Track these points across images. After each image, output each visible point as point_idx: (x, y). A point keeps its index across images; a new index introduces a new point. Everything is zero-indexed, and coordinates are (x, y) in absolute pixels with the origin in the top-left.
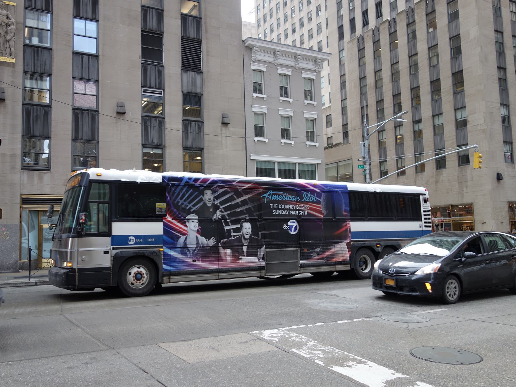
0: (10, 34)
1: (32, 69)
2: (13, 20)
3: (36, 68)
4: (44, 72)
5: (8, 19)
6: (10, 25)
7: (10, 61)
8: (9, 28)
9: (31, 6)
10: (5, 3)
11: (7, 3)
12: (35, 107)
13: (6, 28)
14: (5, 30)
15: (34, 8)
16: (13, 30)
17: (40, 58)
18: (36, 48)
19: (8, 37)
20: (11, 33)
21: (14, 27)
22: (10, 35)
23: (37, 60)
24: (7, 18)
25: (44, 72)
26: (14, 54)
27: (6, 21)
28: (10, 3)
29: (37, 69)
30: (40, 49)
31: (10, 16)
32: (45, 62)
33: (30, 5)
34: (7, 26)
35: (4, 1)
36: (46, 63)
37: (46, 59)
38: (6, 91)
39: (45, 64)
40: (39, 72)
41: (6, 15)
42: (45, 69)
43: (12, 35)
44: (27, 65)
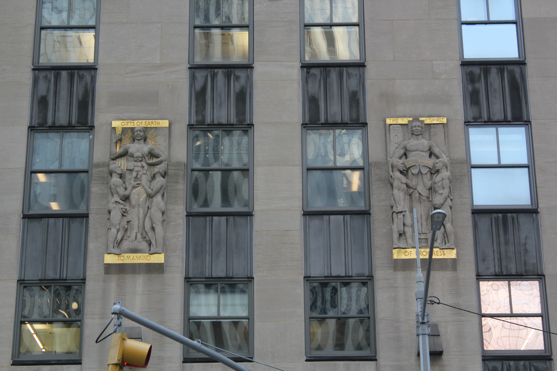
0: (440, 192)
1: (497, 267)
2: (444, 158)
3: (504, 264)
4: (526, 271)
5: (433, 157)
6: (438, 171)
7: (445, 257)
8: (438, 178)
9: (480, 117)
10: (423, 121)
11: (428, 121)
12: (512, 363)
13: (431, 179)
14: (429, 184)
15: (486, 120)
16: (446, 182)
17: (511, 237)
18: (500, 215)
19: (438, 199)
20: (443, 188)
21: (448, 173)
22: (442, 194)
23: (507, 243)
24: (431, 154)
25: (526, 271)
26: (452, 238)
27: (430, 162)
28: (435, 121)
29: (507, 267)
30: (509, 215)
31: (436, 150)
32: (525, 244)
33: (478, 116)
34: (431, 173)
35: (421, 119)
36: (528, 246)
37: (526, 238)
38: (442, 330)
39: (526, 251)
40: (514, 273)
41: (428, 148)
42: (525, 264)
43: (446, 192)
44: (484, 260)
